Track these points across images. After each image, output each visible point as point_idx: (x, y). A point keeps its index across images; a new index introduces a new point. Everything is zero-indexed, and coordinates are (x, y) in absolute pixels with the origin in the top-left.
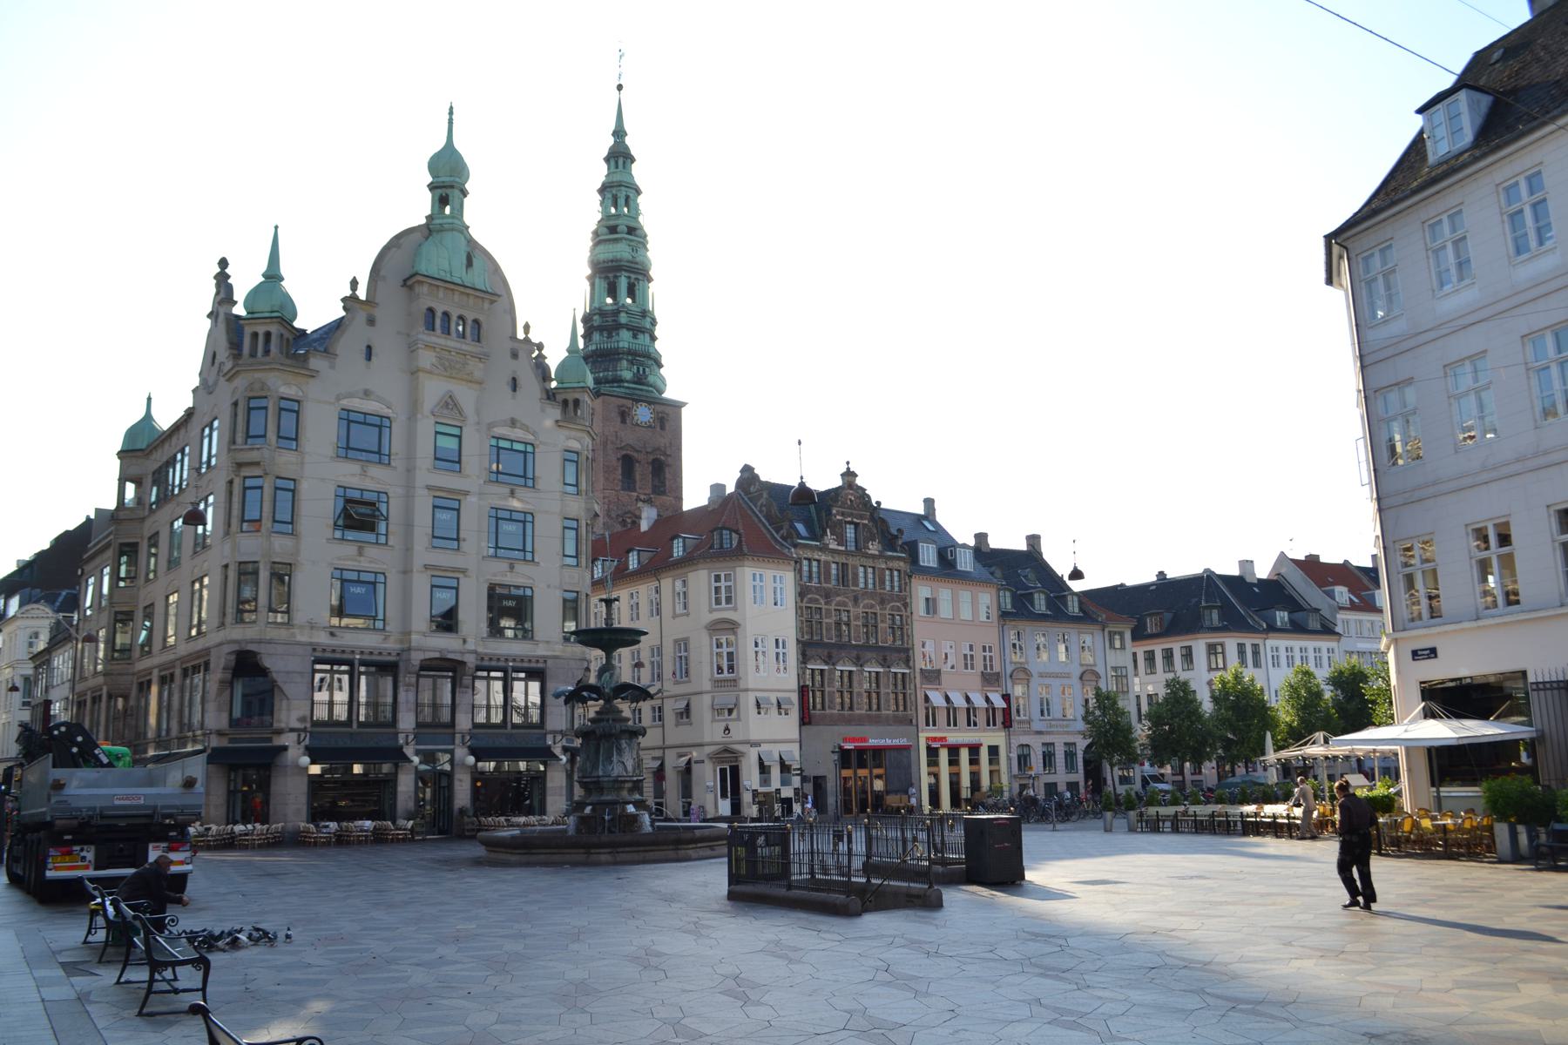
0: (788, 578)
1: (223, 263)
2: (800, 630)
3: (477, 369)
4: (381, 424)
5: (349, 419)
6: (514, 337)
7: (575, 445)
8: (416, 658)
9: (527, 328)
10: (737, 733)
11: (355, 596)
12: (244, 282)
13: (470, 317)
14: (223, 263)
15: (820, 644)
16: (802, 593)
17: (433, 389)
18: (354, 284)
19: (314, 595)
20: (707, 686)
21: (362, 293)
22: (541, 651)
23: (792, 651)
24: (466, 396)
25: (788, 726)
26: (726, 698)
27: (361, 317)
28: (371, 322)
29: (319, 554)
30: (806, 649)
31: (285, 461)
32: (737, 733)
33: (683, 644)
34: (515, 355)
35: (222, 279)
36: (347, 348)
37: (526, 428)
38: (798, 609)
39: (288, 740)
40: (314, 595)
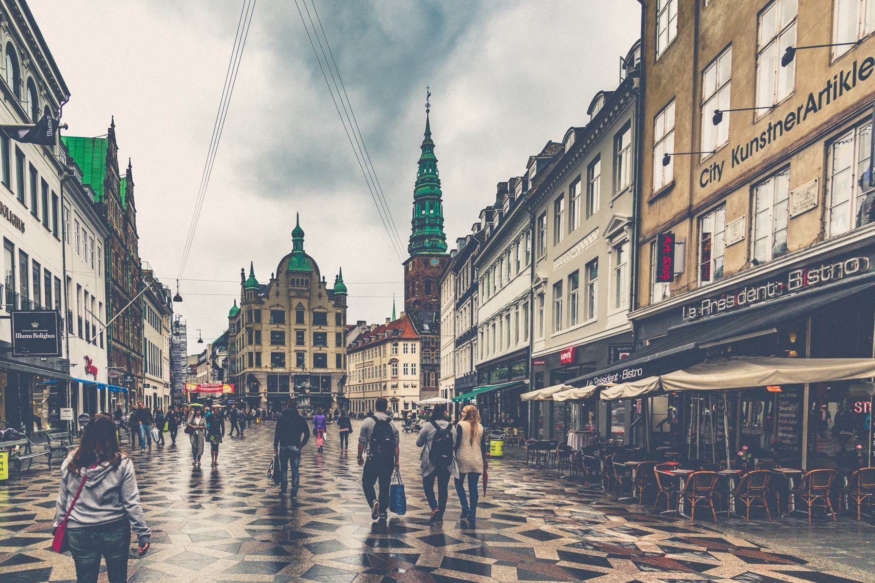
0: (418, 345)
1: (243, 270)
2: (422, 361)
3: (307, 294)
4: (283, 313)
5: (273, 313)
6: (319, 282)
7: (339, 311)
8: (293, 374)
9: (324, 278)
10: (398, 393)
11: (278, 359)
12: (247, 278)
13: (305, 279)
14: (243, 270)
15: (429, 365)
16: (422, 349)
17: (295, 302)
18: (273, 275)
19: (266, 360)
20: (390, 379)
21: (275, 277)
22: (330, 371)
23: (418, 368)
24: (305, 302)
25: (417, 391)
26: (395, 383)
27: (275, 284)
28: (278, 285)
29: (267, 350)
30: (422, 366)
31: (257, 327)
32: (398, 393)
33: (385, 365)
34: (320, 287)
35: (243, 274)
36: (272, 293)
37: (324, 308)
38: (421, 354)
39: (262, 395)
40: (266, 360)
